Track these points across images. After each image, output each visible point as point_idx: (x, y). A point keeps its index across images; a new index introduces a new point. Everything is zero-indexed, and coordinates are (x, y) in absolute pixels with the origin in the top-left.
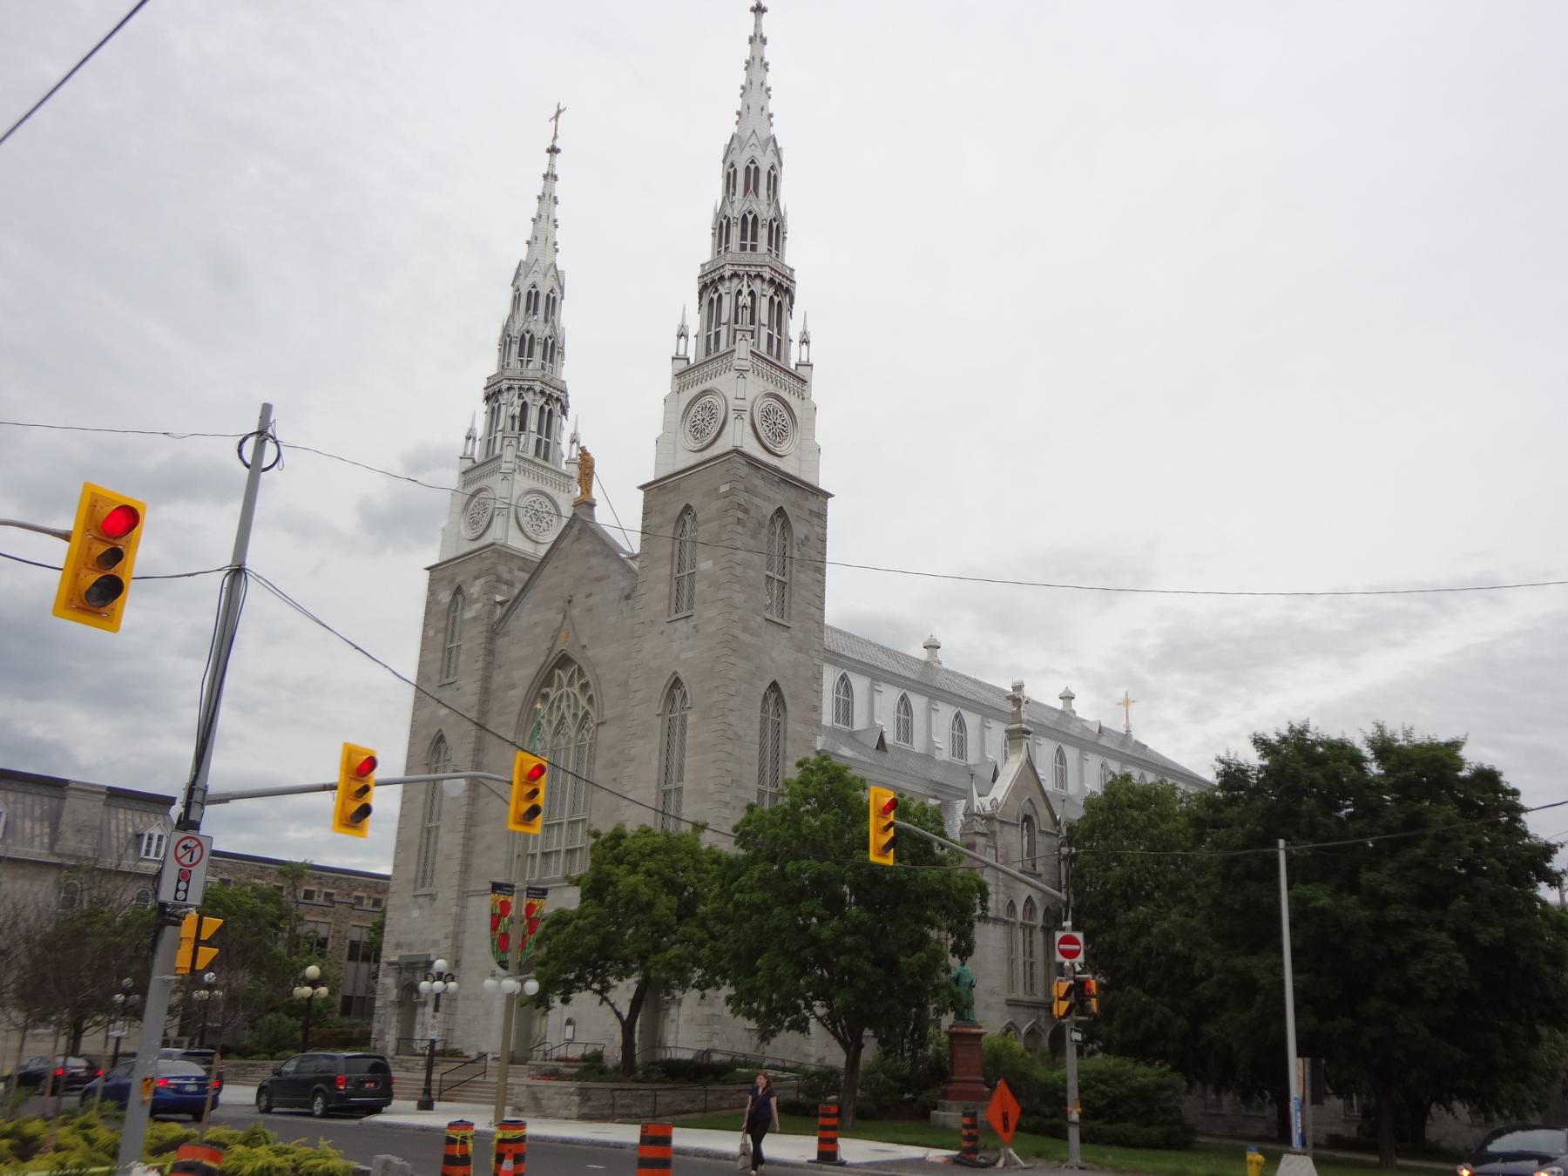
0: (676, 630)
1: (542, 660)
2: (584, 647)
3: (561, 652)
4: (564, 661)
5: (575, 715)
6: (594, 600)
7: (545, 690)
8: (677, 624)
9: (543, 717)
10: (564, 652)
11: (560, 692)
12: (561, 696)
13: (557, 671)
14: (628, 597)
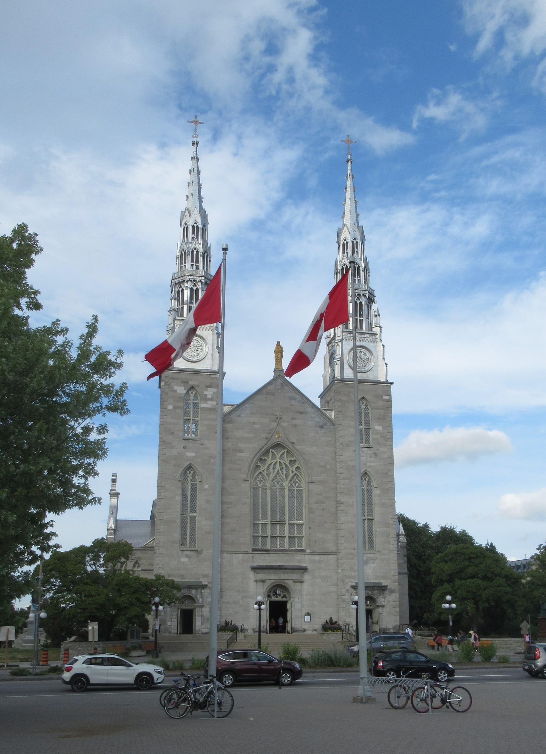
0: (363, 452)
1: (263, 442)
2: (293, 443)
3: (277, 442)
4: (278, 446)
5: (287, 475)
6: (296, 422)
7: (263, 458)
8: (364, 449)
9: (264, 471)
10: (279, 442)
11: (275, 461)
12: (277, 462)
13: (271, 450)
14: (322, 427)
